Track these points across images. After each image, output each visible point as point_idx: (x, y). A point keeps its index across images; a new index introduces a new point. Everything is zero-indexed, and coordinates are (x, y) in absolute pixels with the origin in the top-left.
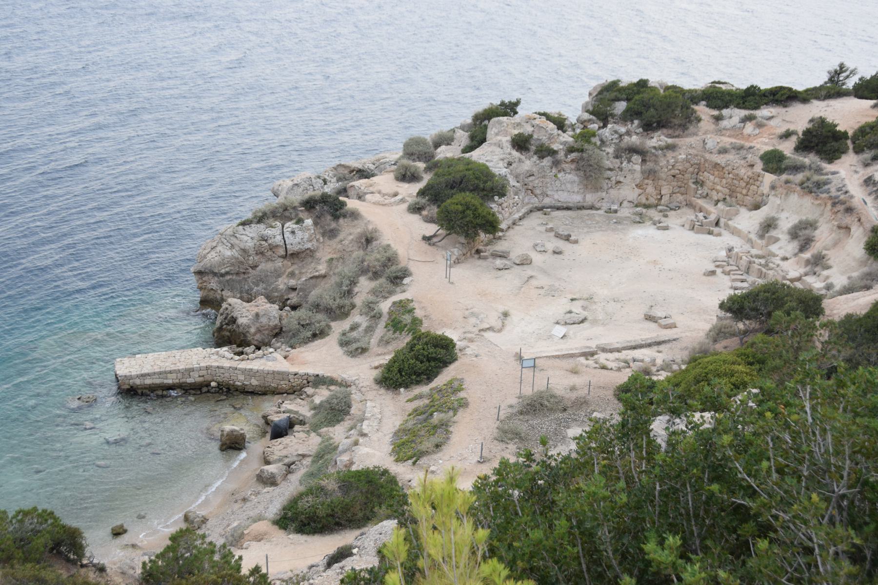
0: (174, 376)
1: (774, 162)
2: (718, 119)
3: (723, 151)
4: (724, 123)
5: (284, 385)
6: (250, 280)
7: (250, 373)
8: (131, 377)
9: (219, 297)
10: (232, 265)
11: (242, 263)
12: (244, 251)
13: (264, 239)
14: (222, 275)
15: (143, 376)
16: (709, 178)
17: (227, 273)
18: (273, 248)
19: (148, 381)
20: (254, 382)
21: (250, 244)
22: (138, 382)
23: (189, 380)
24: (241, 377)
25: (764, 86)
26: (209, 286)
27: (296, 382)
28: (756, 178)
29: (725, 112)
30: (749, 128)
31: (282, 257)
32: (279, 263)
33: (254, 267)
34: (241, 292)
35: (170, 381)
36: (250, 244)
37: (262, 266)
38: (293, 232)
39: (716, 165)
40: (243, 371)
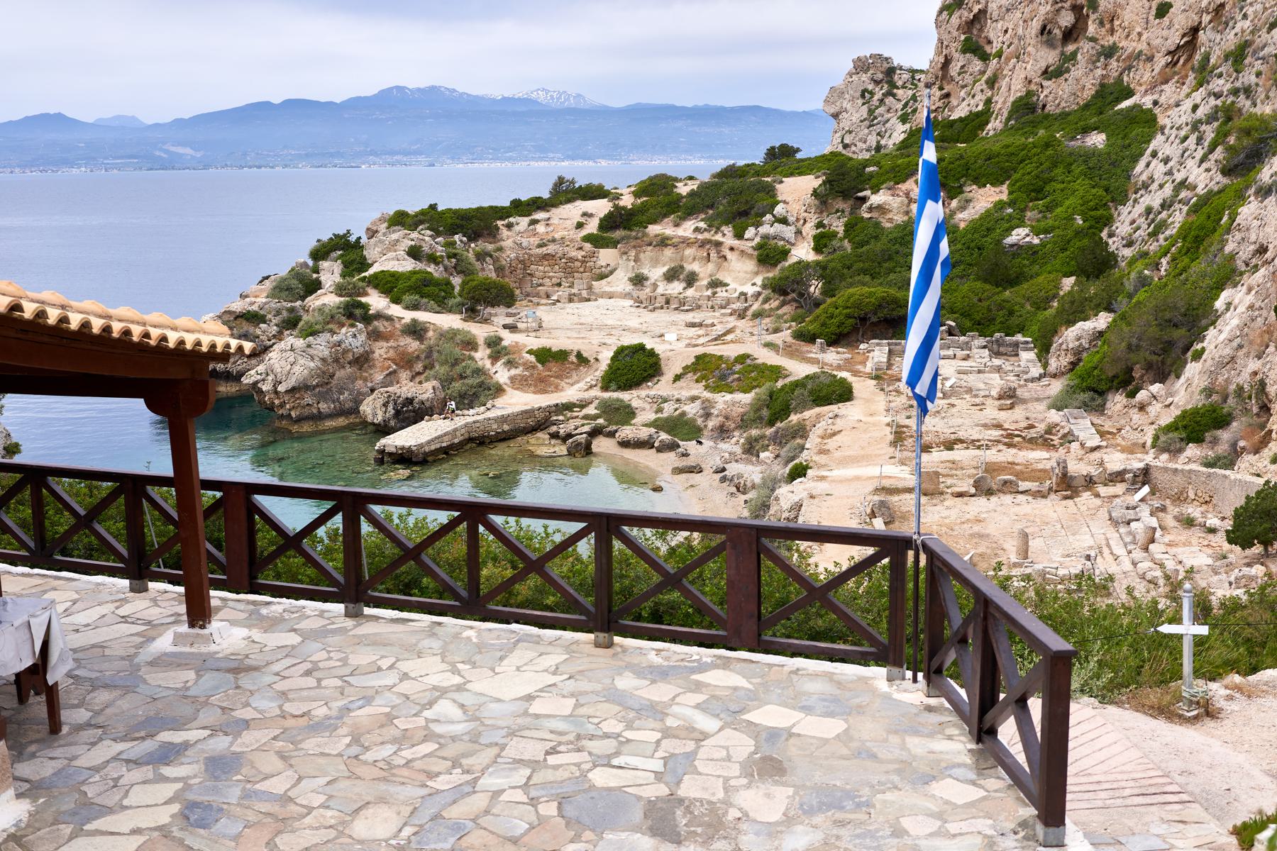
0: (446, 438)
1: (597, 241)
2: (509, 226)
3: (540, 246)
4: (517, 228)
5: (531, 422)
6: (334, 390)
7: (504, 419)
8: (421, 446)
9: (315, 411)
10: (318, 376)
11: (324, 373)
12: (323, 360)
13: (339, 344)
14: (314, 387)
15: (429, 442)
16: (538, 270)
17: (317, 385)
18: (345, 352)
19: (433, 448)
20: (506, 427)
21: (326, 353)
22: (427, 449)
23: (456, 441)
24: (495, 426)
25: (524, 198)
26: (304, 402)
27: (540, 416)
28: (593, 255)
29: (511, 219)
30: (541, 228)
31: (349, 363)
32: (349, 370)
33: (332, 376)
34: (334, 402)
35: (444, 445)
36: (326, 353)
37: (338, 374)
38: (354, 336)
39: (545, 257)
40: (496, 419)
